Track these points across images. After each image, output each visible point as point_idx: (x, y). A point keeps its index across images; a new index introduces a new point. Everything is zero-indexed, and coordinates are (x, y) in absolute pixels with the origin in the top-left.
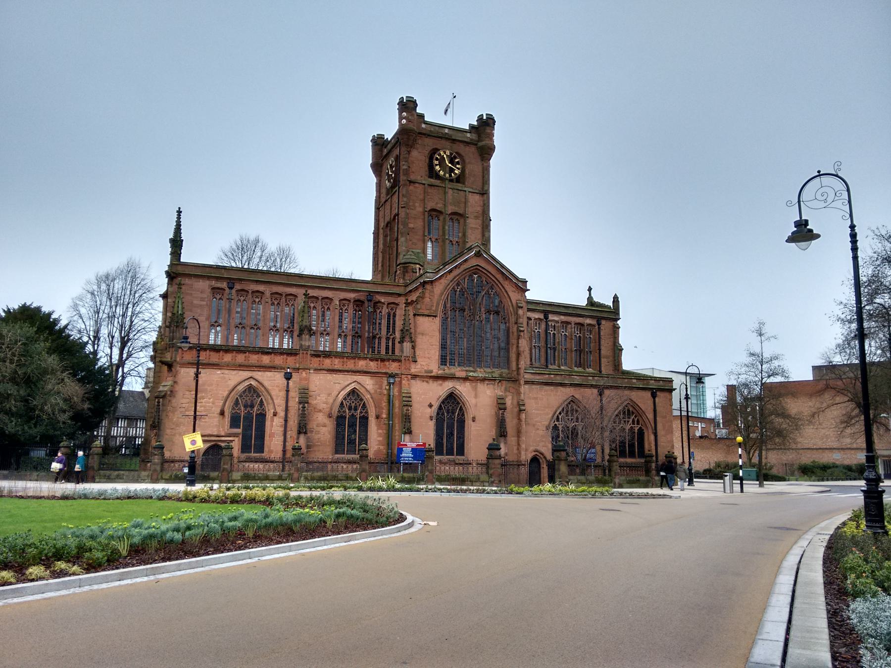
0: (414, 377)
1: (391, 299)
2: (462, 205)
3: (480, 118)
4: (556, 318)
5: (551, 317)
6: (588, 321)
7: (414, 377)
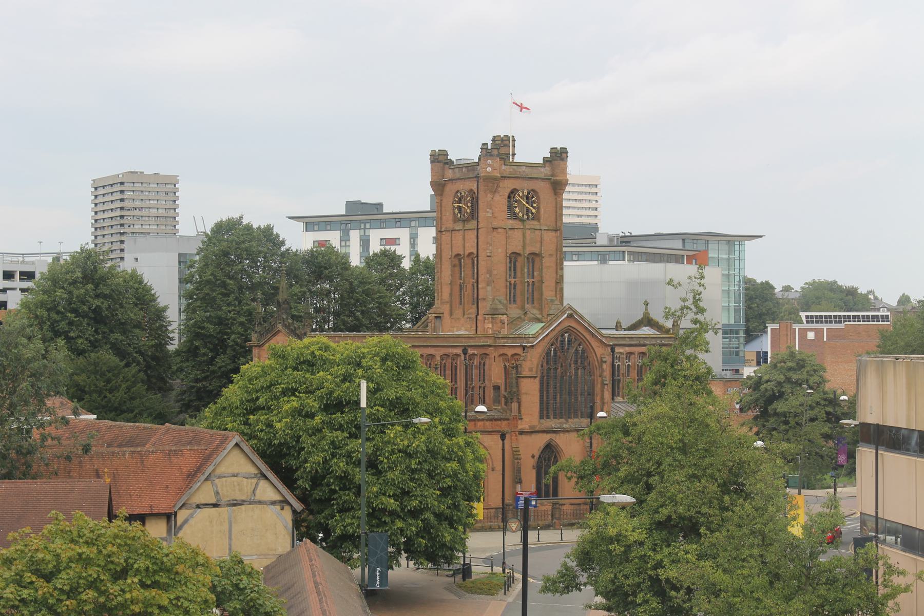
0: (522, 433)
1: (483, 351)
2: (538, 245)
3: (554, 151)
4: (621, 350)
7: (522, 433)
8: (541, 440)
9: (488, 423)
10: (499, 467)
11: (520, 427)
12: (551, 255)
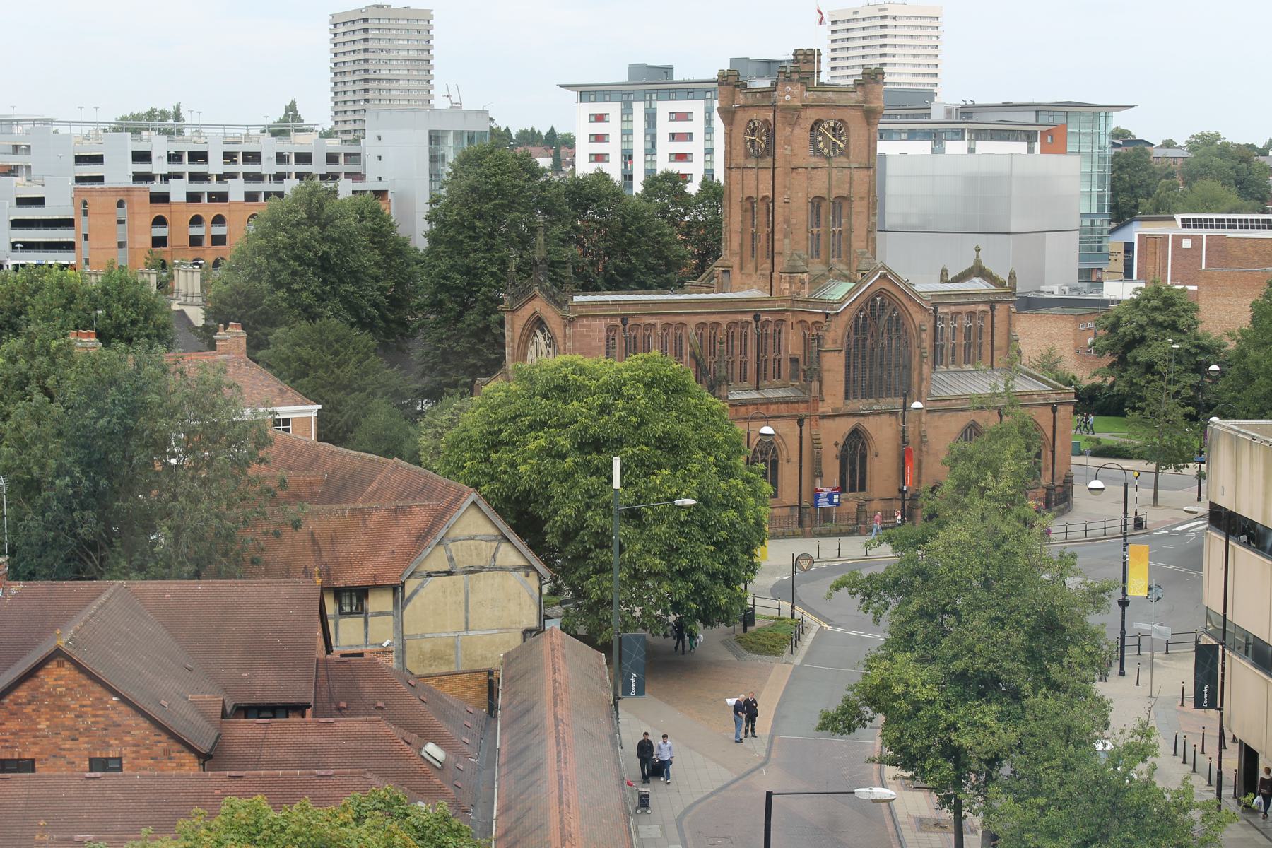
2: (847, 186)
5: (941, 310)
6: (981, 308)
7: (823, 417)
8: (847, 425)
9: (782, 406)
10: (796, 459)
11: (821, 410)
12: (862, 198)
